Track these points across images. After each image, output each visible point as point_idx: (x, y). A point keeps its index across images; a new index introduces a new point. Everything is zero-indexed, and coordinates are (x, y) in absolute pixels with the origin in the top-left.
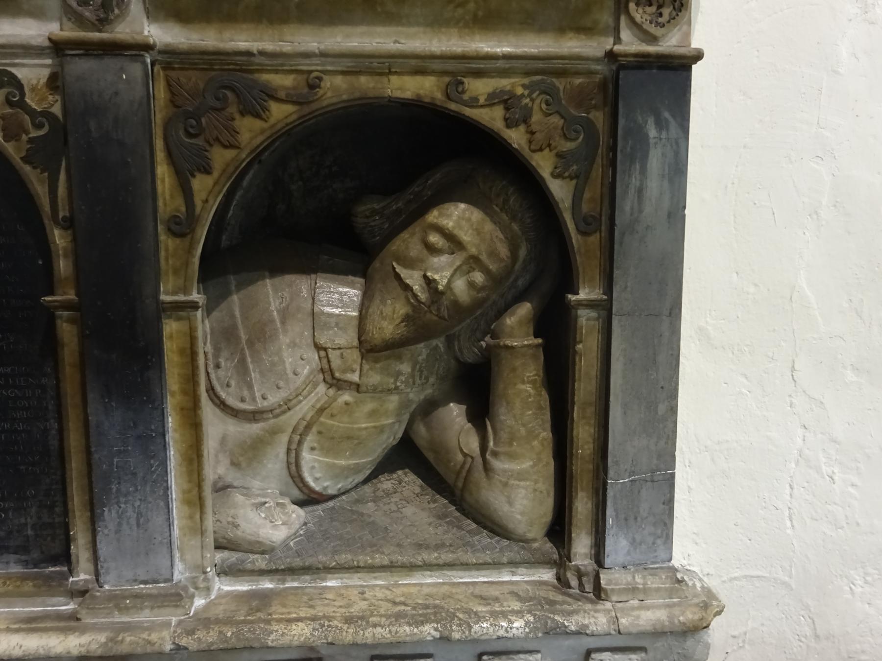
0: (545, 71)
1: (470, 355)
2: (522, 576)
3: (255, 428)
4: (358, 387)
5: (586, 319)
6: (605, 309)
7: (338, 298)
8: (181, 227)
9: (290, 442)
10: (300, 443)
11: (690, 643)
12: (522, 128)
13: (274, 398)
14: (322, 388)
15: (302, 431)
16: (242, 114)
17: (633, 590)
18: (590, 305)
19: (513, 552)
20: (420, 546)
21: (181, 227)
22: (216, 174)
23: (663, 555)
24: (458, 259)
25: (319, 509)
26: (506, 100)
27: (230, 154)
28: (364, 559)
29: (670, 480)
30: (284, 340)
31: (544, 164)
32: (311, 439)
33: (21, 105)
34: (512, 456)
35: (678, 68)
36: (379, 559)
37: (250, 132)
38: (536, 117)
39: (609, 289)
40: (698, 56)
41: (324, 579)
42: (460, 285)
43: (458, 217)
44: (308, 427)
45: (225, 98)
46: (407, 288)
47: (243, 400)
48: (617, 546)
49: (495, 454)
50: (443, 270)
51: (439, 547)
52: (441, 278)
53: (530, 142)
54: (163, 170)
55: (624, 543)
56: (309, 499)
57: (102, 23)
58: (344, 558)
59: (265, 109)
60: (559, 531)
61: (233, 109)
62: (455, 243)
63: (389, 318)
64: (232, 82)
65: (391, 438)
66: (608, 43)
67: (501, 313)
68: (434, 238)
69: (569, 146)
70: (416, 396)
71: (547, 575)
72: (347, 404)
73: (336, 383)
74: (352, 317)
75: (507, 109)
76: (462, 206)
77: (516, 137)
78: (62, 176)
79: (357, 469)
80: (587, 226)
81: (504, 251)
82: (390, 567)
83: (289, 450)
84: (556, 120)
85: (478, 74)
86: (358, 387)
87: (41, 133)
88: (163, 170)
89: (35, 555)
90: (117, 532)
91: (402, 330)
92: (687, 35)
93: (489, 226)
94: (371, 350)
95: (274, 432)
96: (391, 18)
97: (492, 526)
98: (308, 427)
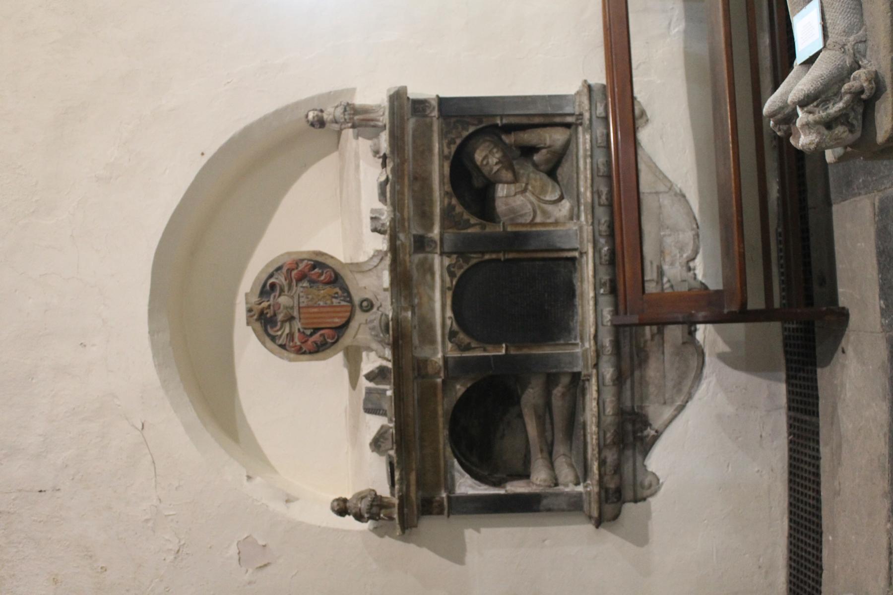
0: (443, 135)
1: (518, 153)
2: (581, 136)
3: (538, 212)
4: (527, 184)
5: (505, 121)
6: (502, 116)
7: (502, 191)
8: (483, 227)
11: (595, 89)
13: (530, 206)
15: (540, 200)
17: (580, 105)
18: (501, 120)
19: (574, 140)
20: (572, 165)
21: (483, 227)
24: (490, 156)
25: (565, 196)
26: (449, 145)
28: (575, 181)
29: (550, 96)
30: (513, 204)
31: (465, 134)
32: (542, 197)
33: (455, 264)
34: (545, 140)
35: (443, 102)
36: (575, 175)
37: (459, 209)
38: (453, 136)
39: (497, 115)
40: (438, 96)
42: (497, 155)
43: (478, 157)
46: (498, 170)
48: (568, 110)
50: (493, 160)
52: (495, 160)
54: (469, 231)
56: (561, 198)
57: (435, 242)
58: (575, 186)
60: (568, 126)
62: (486, 157)
63: (507, 175)
64: (447, 213)
65: (545, 177)
66: (435, 119)
67: (505, 143)
68: (485, 163)
70: (531, 168)
71: (580, 129)
73: (524, 191)
77: (458, 141)
78: (472, 255)
79: (553, 187)
80: (480, 122)
81: (487, 144)
82: (578, 174)
84: (454, 131)
85: (443, 151)
86: (527, 184)
88: (469, 231)
93: (481, 148)
94: (516, 180)
95: (539, 207)
96: (430, 174)
97: (567, 145)
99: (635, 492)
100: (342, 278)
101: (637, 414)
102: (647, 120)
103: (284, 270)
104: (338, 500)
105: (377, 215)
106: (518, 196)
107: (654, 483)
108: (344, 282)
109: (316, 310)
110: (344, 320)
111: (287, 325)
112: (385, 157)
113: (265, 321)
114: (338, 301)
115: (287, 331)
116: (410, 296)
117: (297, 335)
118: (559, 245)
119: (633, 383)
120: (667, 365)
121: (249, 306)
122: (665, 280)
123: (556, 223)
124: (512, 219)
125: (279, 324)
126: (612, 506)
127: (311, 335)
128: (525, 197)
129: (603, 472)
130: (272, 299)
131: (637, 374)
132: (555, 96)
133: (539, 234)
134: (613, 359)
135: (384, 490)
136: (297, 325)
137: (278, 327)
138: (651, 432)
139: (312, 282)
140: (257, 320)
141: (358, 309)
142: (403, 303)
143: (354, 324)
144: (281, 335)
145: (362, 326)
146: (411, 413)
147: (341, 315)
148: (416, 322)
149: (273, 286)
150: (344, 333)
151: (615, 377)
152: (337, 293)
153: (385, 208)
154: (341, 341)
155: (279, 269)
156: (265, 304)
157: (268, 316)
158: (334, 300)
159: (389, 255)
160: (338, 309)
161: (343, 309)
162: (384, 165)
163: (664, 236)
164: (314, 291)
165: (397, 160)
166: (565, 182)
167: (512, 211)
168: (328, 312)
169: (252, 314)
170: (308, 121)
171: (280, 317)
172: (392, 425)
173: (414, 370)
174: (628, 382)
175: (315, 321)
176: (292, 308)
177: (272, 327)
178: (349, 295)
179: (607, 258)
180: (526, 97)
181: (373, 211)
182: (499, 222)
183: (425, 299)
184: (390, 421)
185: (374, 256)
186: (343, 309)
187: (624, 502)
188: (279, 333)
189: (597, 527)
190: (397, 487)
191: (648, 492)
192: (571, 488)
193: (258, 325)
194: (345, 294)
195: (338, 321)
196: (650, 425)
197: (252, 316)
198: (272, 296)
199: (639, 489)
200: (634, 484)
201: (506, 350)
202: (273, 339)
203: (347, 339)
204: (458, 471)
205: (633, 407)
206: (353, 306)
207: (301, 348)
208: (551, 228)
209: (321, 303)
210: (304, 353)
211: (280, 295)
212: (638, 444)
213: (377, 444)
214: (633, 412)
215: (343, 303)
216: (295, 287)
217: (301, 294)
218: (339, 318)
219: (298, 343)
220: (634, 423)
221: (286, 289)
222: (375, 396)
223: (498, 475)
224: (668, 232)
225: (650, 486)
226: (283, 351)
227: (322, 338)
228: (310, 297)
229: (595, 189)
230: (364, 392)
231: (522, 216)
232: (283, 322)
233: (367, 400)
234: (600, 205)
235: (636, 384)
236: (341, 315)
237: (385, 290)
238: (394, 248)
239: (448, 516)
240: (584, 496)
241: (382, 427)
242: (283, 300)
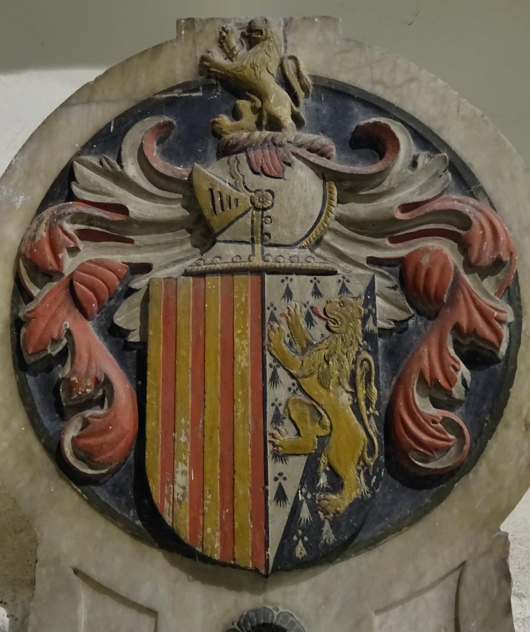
100: (420, 513)
103: (466, 205)
108: (398, 528)
109: (243, 359)
110: (178, 517)
111: (173, 211)
113: (202, 108)
115: (139, 208)
117: (118, 256)
121: (276, 29)
125: (180, 171)
127: (114, 333)
130: (307, 137)
136: (168, 260)
137: (159, 163)
139: (394, 346)
140: (205, 67)
141: (245, 602)
143: (153, 575)
144: (121, 179)
145: (147, 621)
149: (374, 143)
150: (104, 510)
152: (336, 483)
154: (70, 497)
155: (462, 176)
156: (281, 105)
157: (225, 120)
158: (295, 467)
160: (243, 489)
161: (244, 518)
169: (234, 41)
171: (214, 174)
175: (185, 353)
176: (260, 236)
177: (163, 133)
178: (323, 556)
186: (244, 518)
188: (132, 170)
193: (177, 68)
194: (328, 534)
195: (175, 488)
197: (222, 42)
198: (323, 140)
202: (107, 140)
206: (261, 577)
207: (44, 274)
209: (279, 394)
210: (20, 293)
211: (325, 175)
215: (278, 518)
216: (364, 253)
217: (330, 285)
218: (198, 487)
219: (70, 264)
221: (360, 210)
226: (40, 191)
227: (87, 388)
228: (319, 329)
232: (187, 189)
236: (212, 498)
242: (301, 193)
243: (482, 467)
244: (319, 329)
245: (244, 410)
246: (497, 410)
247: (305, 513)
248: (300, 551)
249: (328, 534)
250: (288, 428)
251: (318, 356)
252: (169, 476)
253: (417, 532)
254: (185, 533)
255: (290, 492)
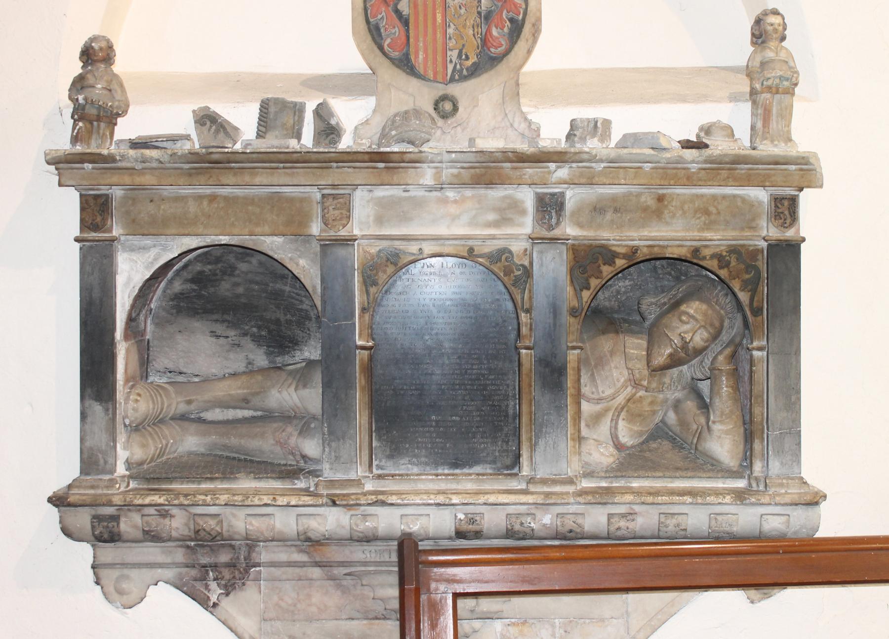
8: (573, 312)
9: (613, 415)
10: (618, 416)
12: (726, 270)
14: (629, 389)
16: (604, 264)
22: (591, 290)
23: (797, 471)
26: (719, 257)
27: (599, 280)
31: (736, 285)
32: (623, 414)
38: (733, 263)
40: (804, 240)
41: (631, 483)
44: (622, 409)
45: (597, 259)
47: (593, 393)
49: (714, 422)
51: (687, 469)
53: (730, 275)
55: (777, 464)
59: (614, 263)
61: (600, 262)
68: (684, 318)
69: (747, 276)
72: (640, 397)
74: (642, 355)
75: (719, 261)
76: (697, 303)
77: (723, 273)
79: (640, 434)
83: (612, 420)
87: (520, 273)
89: (499, 465)
90: (545, 451)
91: (668, 361)
92: (798, 230)
95: (607, 410)
98: (622, 409)
99: (112, 566)
101: (247, 571)
102: (752, 602)
104: (110, 47)
105: (600, 131)
106: (626, 372)
107: (125, 599)
108: (486, 71)
110: (420, 69)
112: (699, 145)
114: (454, 59)
116: (459, 183)
118: (542, 443)
119: (302, 565)
120: (331, 625)
122: (477, 624)
123: (579, 439)
124: (587, 362)
126: (89, 527)
128: (624, 386)
129: (147, 511)
131: (316, 572)
132: (799, 444)
133: (560, 409)
134: (345, 533)
135: (127, 129)
138: (215, 592)
142: (448, 173)
146: (257, 180)
147: (430, 63)
148: (415, 192)
151: (310, 534)
152: (467, 58)
153: (612, 145)
158: (455, 53)
159: (532, 150)
160: (439, 59)
161: (440, 68)
162: (687, 145)
163: (553, 626)
164: (473, 18)
165: (694, 167)
166: (648, 454)
167: (601, 363)
168: (435, 40)
170: (766, 14)
172: (238, 147)
173: (334, 186)
174: (304, 558)
175: (421, 18)
179: (517, 527)
180: (798, 392)
181: (607, 123)
182: (582, 341)
183: (453, 209)
184: (247, 144)
185: (530, 123)
187: (93, 546)
189: (50, 500)
190: (132, 152)
191: (111, 589)
192: (122, 454)
194: (465, 72)
196: (227, 594)
199: (115, 573)
200: (124, 565)
201: (363, 348)
203: (389, 74)
204: (156, 259)
205: (259, 565)
208: (570, 430)
209: (450, 31)
212: (194, 572)
213: (207, 120)
214: (251, 564)
215: (450, 68)
218: (426, 59)
220: (232, 565)
222: (289, 120)
223: (150, 327)
224: (559, 632)
225: (121, 592)
228: (463, 11)
229: (637, 508)
230: (298, 100)
231: (593, 378)
233: (283, 105)
234: (610, 516)
235: (297, 570)
236: (430, 63)
237: (472, 141)
238: (542, 158)
239: (77, 240)
240: (107, 477)
241: (236, 129)
243: (513, 53)
244: (463, 11)
245: (439, 35)
246: (518, 36)
247: (458, 67)
248: (457, 77)
249: (465, 72)
250: (453, 40)
251: (462, 19)
252: (417, 56)
253: (492, 72)
254: (422, 72)
255: (454, 59)
